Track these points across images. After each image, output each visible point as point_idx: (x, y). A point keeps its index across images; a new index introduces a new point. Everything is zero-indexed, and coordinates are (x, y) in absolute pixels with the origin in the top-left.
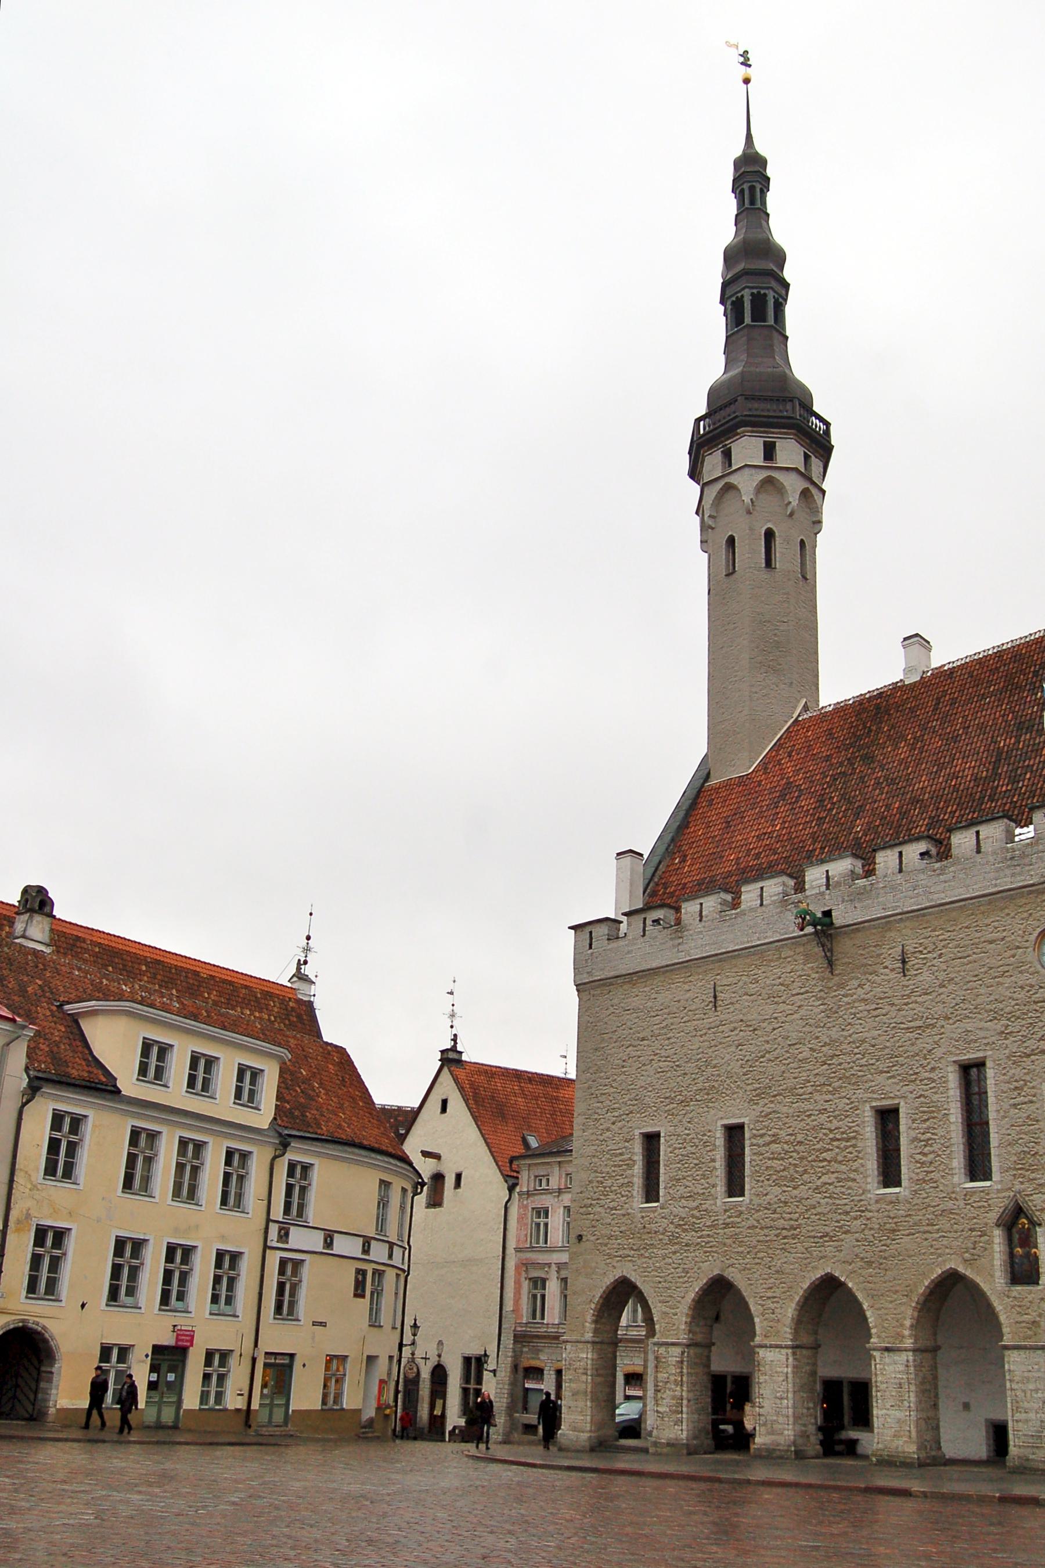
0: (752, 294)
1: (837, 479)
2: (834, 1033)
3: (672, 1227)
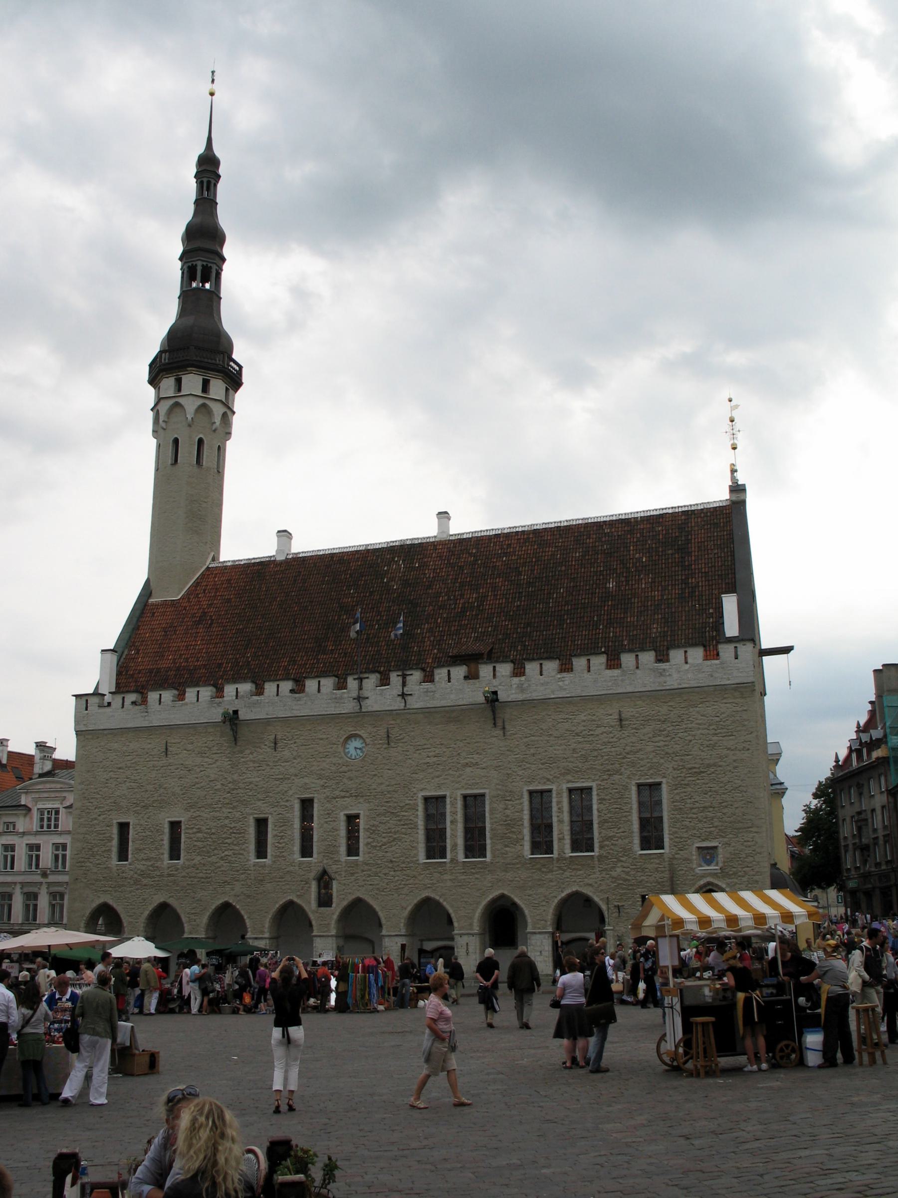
0: (203, 265)
1: (241, 400)
2: (235, 777)
3: (136, 876)
